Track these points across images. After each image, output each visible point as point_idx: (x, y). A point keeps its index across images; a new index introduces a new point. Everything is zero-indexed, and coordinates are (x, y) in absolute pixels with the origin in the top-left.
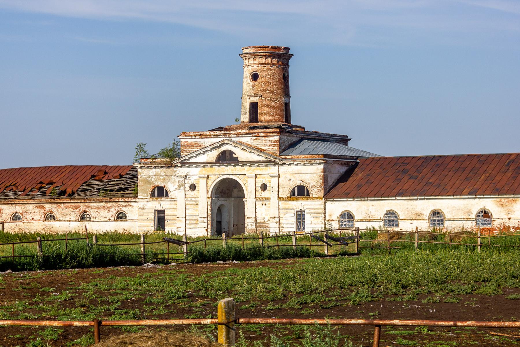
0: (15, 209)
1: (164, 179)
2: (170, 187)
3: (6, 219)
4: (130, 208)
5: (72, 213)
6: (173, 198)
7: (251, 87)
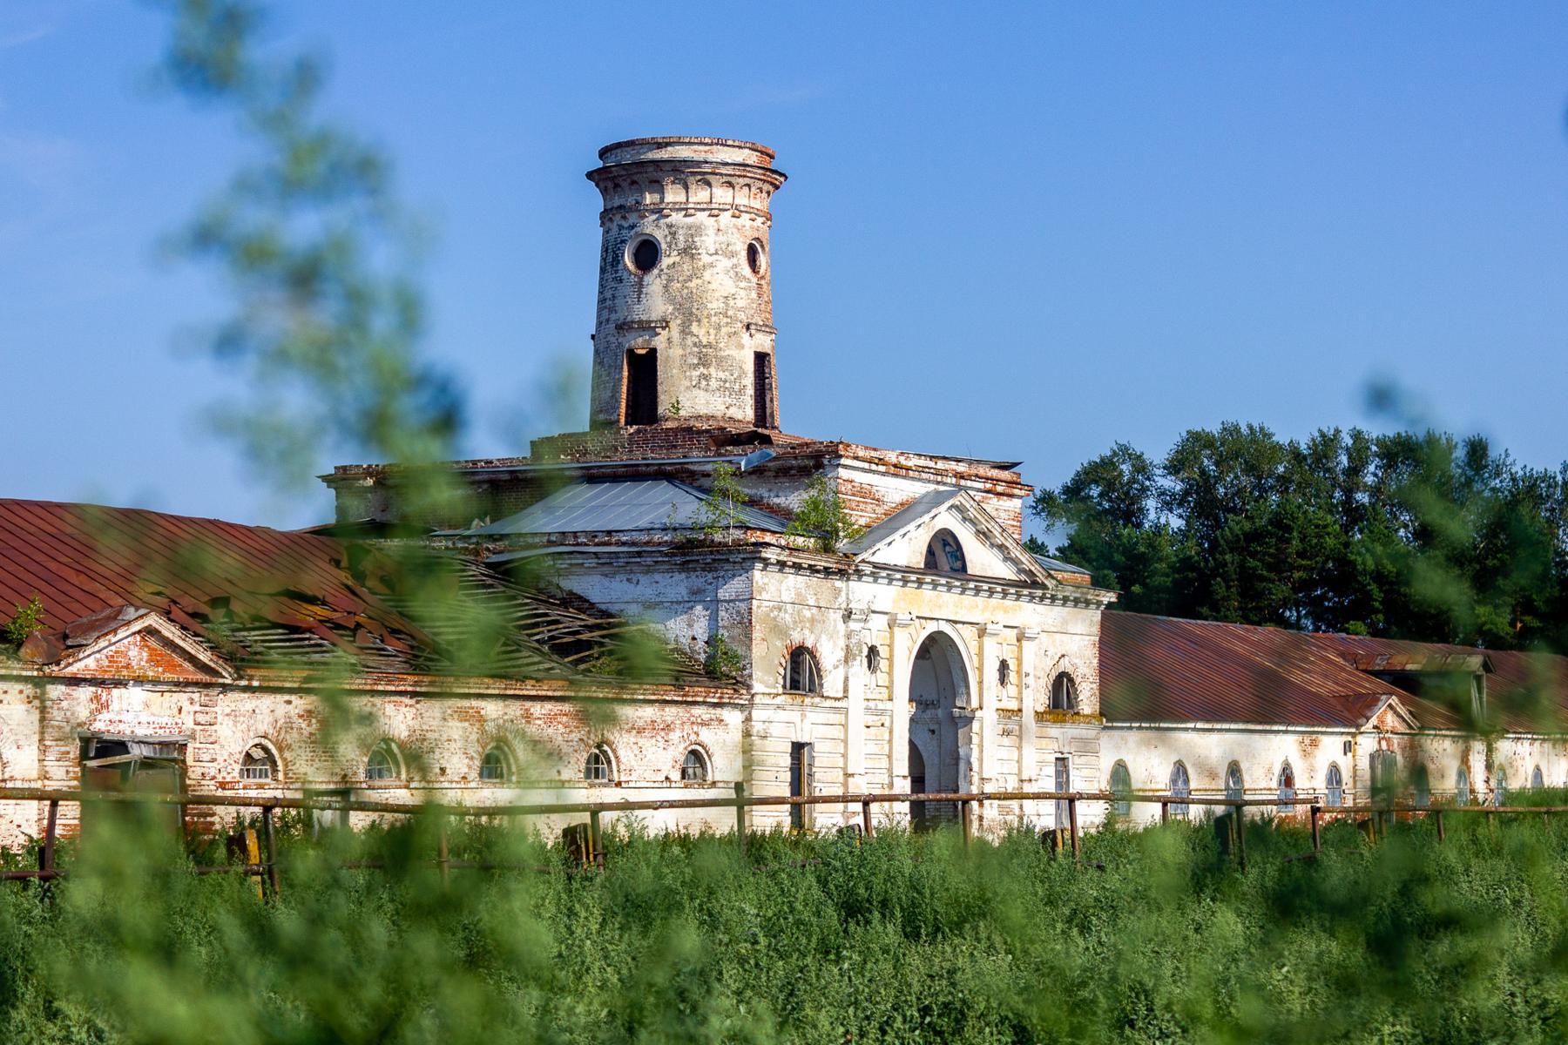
1: (813, 620)
2: (829, 654)
4: (720, 731)
7: (754, 295)
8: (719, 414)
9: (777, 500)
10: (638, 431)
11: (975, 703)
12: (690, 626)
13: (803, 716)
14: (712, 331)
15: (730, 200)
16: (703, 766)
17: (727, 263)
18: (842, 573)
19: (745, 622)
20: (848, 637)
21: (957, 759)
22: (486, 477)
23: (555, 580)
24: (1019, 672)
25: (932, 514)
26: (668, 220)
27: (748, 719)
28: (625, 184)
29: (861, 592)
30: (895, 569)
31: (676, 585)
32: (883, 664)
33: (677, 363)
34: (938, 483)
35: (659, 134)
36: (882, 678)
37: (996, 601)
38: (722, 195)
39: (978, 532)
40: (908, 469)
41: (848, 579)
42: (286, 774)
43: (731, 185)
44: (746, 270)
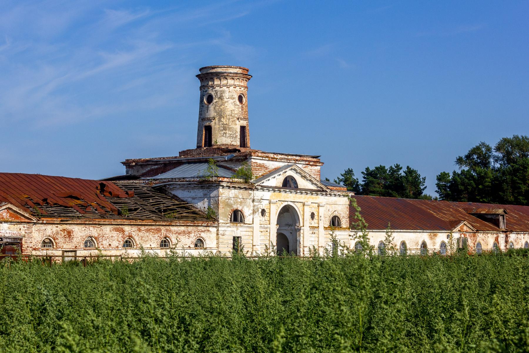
0: (89, 231)
1: (241, 202)
2: (247, 212)
3: (78, 246)
4: (208, 234)
5: (153, 239)
6: (249, 224)
7: (240, 110)
8: (229, 144)
9: (236, 168)
10: (206, 149)
11: (301, 225)
12: (204, 204)
13: (237, 229)
14: (227, 120)
15: (233, 83)
16: (203, 243)
17: (232, 101)
18: (251, 189)
19: (217, 203)
20: (254, 206)
21: (297, 240)
22: (163, 162)
23: (170, 191)
24: (318, 216)
25: (284, 171)
26: (215, 89)
27: (218, 230)
28: (204, 79)
29: (258, 194)
30: (271, 187)
31: (200, 193)
32: (267, 214)
33: (217, 130)
34: (289, 163)
35: (212, 65)
36: (266, 218)
37: (309, 195)
38: (231, 82)
39: (302, 176)
40: (277, 159)
41: (254, 190)
42: (56, 246)
43: (233, 79)
44: (238, 103)
